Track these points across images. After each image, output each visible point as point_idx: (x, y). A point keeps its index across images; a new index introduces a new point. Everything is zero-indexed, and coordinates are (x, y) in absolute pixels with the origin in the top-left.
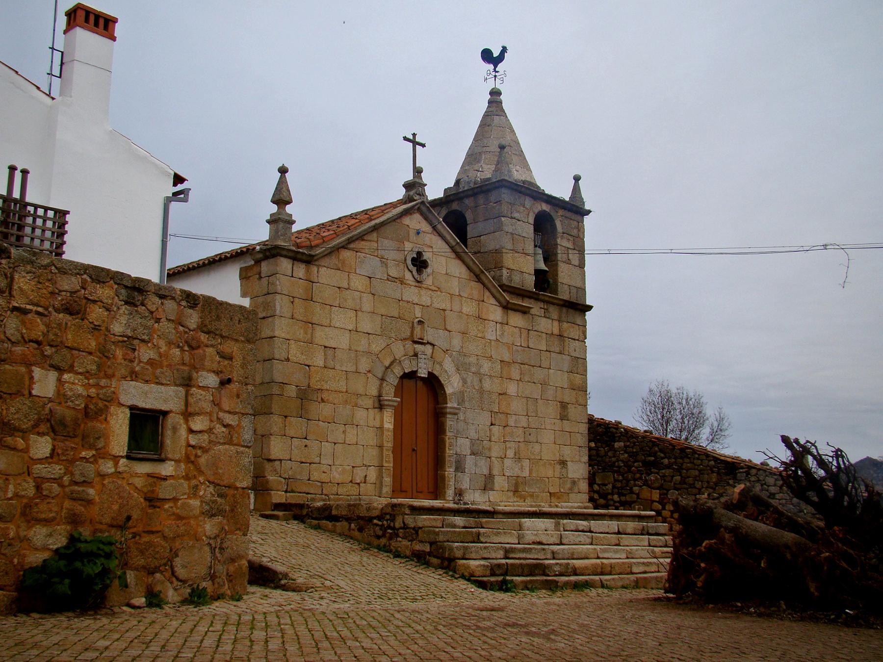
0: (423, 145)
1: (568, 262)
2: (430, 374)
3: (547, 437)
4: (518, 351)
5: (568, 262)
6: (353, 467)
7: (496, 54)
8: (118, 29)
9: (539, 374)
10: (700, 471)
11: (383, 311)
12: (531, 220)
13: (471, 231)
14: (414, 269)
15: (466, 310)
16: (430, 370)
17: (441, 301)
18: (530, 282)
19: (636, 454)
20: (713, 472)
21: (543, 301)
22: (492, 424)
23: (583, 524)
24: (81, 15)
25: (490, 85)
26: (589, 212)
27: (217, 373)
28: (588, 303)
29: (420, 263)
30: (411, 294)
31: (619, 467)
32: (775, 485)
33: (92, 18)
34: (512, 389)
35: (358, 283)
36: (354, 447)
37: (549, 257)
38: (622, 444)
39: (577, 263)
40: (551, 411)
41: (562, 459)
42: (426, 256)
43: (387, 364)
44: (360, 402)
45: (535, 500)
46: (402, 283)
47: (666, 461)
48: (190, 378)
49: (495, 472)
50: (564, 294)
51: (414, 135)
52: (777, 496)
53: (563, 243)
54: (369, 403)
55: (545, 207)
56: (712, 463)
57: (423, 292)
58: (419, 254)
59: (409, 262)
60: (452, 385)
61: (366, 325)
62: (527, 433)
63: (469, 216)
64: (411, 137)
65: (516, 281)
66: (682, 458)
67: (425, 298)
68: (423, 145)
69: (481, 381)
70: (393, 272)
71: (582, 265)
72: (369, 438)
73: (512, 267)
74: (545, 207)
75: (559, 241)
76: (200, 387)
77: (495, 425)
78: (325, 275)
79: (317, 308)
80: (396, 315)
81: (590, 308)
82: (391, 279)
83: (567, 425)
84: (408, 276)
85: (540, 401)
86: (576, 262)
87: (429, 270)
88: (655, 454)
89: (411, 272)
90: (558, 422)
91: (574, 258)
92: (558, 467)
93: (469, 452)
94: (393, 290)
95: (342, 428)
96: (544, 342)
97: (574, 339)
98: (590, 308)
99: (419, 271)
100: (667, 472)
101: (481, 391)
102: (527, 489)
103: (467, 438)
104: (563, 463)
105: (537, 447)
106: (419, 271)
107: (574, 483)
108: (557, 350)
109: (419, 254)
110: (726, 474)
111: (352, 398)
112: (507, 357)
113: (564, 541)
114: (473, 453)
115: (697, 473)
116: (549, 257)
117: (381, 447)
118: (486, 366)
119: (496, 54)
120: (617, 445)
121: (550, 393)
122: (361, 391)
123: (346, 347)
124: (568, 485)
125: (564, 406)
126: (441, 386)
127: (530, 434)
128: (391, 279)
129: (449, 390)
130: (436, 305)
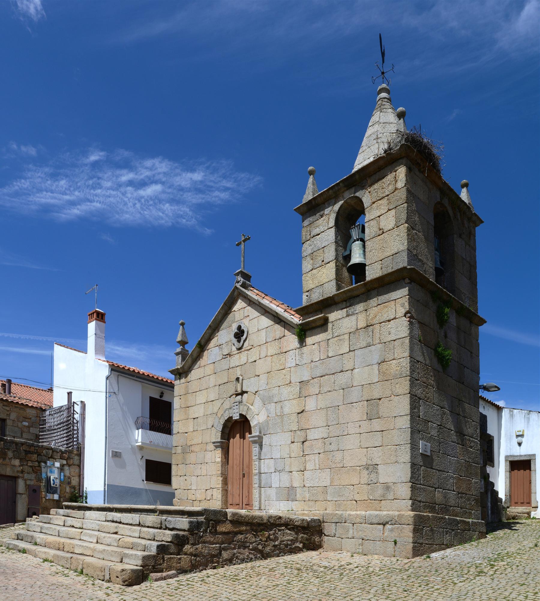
4: (317, 366)
6: (206, 490)
15: (271, 351)
16: (241, 413)
22: (292, 442)
36: (205, 477)
41: (370, 462)
45: (337, 509)
62: (328, 443)
77: (294, 442)
83: (376, 425)
97: (389, 321)
102: (328, 498)
103: (272, 458)
104: (372, 468)
105: (338, 456)
107: (387, 487)
118: (286, 392)
121: (355, 395)
124: (379, 492)
127: (331, 444)
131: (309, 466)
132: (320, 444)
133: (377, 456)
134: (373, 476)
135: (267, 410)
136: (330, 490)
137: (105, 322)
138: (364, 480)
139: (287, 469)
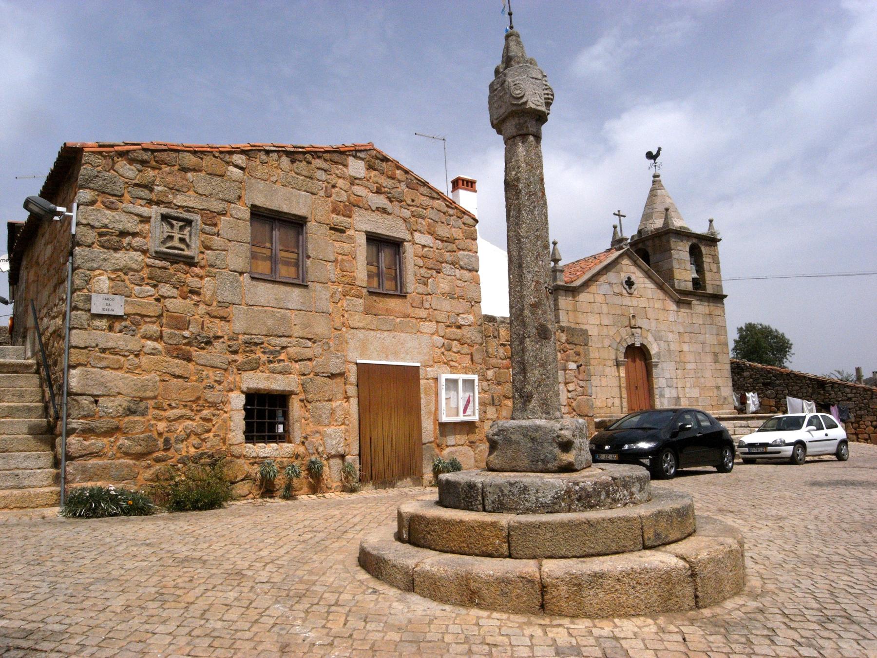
0: (624, 216)
1: (711, 271)
2: (642, 344)
3: (708, 374)
5: (711, 271)
7: (654, 153)
8: (478, 186)
9: (701, 338)
10: (800, 387)
11: (613, 312)
12: (688, 250)
13: (652, 259)
14: (627, 287)
15: (657, 306)
17: (643, 303)
18: (690, 286)
19: (758, 379)
20: (809, 387)
21: (699, 296)
23: (744, 423)
24: (460, 182)
25: (653, 171)
26: (720, 240)
27: (575, 362)
28: (725, 293)
29: (630, 283)
30: (627, 301)
31: (748, 387)
32: (851, 393)
33: (465, 183)
34: (686, 348)
35: (599, 299)
37: (700, 269)
38: (748, 373)
39: (715, 271)
40: (709, 358)
42: (633, 278)
43: (618, 341)
44: (607, 363)
46: (622, 295)
47: (778, 382)
48: (565, 366)
49: (680, 396)
50: (710, 290)
51: (619, 211)
52: (853, 399)
53: (707, 260)
54: (611, 363)
55: (695, 241)
56: (809, 382)
57: (633, 299)
58: (629, 278)
59: (624, 283)
60: (654, 349)
61: (606, 322)
63: (650, 250)
64: (617, 213)
65: (683, 286)
66: (788, 380)
67: (634, 302)
68: (624, 216)
69: (668, 345)
70: (617, 290)
71: (718, 272)
72: (614, 382)
73: (679, 278)
74: (695, 241)
75: (704, 259)
76: (570, 370)
78: (583, 297)
79: (580, 315)
80: (620, 313)
81: (725, 296)
82: (616, 294)
83: (718, 366)
84: (624, 291)
85: (702, 354)
86: (715, 270)
87: (635, 287)
88: (771, 379)
89: (625, 289)
90: (713, 364)
91: (714, 267)
92: (715, 390)
93: (665, 386)
94: (617, 300)
95: (599, 378)
96: (701, 319)
98: (725, 296)
99: (630, 288)
100: (779, 388)
101: (669, 351)
104: (718, 388)
105: (702, 380)
106: (630, 288)
108: (709, 323)
109: (629, 278)
110: (818, 388)
111: (603, 362)
112: (682, 331)
113: (736, 433)
114: (668, 386)
115: (798, 388)
116: (700, 269)
117: (620, 386)
118: (671, 337)
119: (654, 153)
120: (745, 374)
121: (707, 349)
122: (606, 357)
123: (596, 333)
124: (722, 400)
125: (715, 355)
126: (648, 350)
128: (616, 294)
129: (653, 352)
130: (640, 306)
131: (688, 385)
132: (693, 371)
133: (720, 382)
134: (719, 392)
135: (658, 345)
136: (700, 400)
137: (476, 191)
138: (715, 394)
139: (675, 385)
